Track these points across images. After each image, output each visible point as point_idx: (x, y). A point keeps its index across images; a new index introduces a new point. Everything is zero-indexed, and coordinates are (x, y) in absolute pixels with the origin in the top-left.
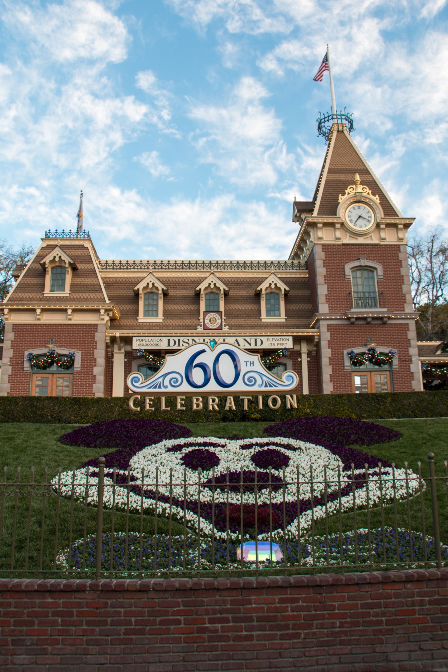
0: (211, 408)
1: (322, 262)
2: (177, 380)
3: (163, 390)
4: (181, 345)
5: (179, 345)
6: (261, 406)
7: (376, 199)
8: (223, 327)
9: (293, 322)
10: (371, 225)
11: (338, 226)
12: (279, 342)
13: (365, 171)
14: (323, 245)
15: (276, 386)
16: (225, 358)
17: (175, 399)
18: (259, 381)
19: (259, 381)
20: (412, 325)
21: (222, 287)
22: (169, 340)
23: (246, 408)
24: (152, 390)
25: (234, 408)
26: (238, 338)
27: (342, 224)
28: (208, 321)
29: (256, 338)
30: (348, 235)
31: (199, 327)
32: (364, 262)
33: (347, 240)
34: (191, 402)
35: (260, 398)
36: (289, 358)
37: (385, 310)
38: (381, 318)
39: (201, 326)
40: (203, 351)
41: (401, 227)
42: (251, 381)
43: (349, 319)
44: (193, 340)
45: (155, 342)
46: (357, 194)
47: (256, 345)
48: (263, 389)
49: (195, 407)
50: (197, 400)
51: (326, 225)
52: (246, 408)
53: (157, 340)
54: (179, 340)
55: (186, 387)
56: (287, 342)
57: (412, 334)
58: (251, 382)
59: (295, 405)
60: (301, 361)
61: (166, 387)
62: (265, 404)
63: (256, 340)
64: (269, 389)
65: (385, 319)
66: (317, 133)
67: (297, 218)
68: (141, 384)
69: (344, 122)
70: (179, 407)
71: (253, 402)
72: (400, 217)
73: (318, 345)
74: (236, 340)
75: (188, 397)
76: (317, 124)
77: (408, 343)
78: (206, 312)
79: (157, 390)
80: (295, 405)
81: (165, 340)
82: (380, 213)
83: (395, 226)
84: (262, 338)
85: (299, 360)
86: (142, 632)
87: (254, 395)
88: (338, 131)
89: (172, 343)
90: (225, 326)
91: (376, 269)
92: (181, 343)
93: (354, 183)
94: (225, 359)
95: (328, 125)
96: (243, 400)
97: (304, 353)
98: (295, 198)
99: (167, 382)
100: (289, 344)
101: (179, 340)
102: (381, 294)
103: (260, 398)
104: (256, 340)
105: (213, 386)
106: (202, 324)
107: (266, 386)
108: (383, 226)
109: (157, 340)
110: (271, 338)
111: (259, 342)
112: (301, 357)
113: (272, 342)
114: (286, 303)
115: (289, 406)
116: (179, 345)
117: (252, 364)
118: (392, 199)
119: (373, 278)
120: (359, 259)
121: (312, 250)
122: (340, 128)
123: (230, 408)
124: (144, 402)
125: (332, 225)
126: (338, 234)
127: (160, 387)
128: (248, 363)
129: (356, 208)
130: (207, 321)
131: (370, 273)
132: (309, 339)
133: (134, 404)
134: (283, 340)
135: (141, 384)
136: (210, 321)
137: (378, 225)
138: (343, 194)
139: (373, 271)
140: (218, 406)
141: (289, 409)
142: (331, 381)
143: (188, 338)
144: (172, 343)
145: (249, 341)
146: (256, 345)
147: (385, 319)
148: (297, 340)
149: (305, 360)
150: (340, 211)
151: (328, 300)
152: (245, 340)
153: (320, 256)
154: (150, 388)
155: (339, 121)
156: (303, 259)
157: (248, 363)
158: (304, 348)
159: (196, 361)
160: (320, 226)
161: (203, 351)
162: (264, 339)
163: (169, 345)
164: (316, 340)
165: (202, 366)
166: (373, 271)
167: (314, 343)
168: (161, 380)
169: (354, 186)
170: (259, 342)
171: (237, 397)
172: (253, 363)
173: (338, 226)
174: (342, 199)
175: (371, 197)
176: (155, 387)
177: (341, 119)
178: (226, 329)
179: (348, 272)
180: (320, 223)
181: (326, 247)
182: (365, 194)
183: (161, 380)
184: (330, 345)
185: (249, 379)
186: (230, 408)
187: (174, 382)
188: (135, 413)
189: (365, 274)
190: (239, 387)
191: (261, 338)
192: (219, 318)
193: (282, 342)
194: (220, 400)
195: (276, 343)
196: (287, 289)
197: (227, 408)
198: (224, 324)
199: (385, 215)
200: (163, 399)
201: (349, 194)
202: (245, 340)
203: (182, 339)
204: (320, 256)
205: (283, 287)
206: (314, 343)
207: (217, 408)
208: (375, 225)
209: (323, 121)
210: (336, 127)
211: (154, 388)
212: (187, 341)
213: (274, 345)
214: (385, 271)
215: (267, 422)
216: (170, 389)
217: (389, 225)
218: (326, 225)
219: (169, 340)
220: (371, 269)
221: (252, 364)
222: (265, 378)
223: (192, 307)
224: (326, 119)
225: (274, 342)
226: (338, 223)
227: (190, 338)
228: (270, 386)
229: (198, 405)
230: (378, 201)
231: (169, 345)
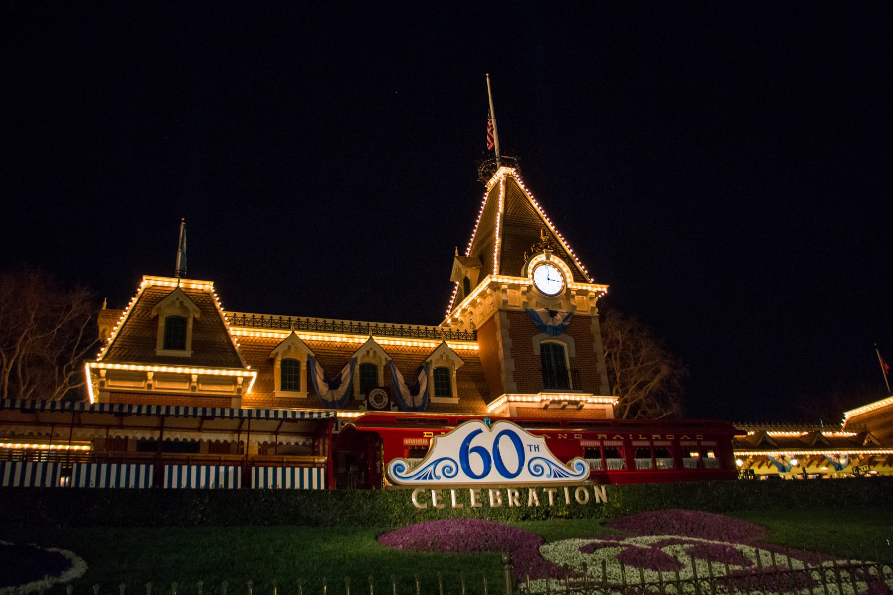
0: (511, 503)
1: (507, 331)
2: (451, 469)
3: (434, 481)
6: (567, 501)
8: (392, 408)
15: (566, 477)
16: (505, 439)
17: (469, 491)
18: (547, 471)
19: (547, 471)
23: (551, 502)
24: (421, 481)
25: (537, 504)
28: (373, 399)
34: (487, 497)
35: (566, 490)
39: (364, 405)
40: (479, 431)
42: (537, 471)
48: (552, 479)
49: (492, 504)
50: (494, 494)
52: (551, 502)
55: (462, 478)
58: (538, 471)
59: (605, 500)
61: (438, 478)
62: (572, 498)
64: (558, 479)
65: (582, 403)
68: (407, 473)
70: (473, 503)
71: (558, 495)
75: (463, 492)
79: (427, 481)
80: (605, 500)
87: (540, 489)
90: (394, 406)
94: (506, 444)
96: (547, 494)
99: (439, 472)
102: (574, 372)
103: (566, 490)
105: (494, 477)
106: (365, 402)
107: (555, 476)
115: (598, 500)
117: (537, 448)
123: (534, 504)
124: (430, 498)
127: (430, 478)
128: (533, 448)
130: (371, 399)
133: (418, 500)
135: (407, 473)
136: (375, 398)
140: (519, 500)
141: (598, 504)
154: (418, 479)
157: (533, 448)
159: (472, 445)
161: (479, 431)
165: (480, 450)
168: (431, 468)
171: (523, 491)
172: (538, 448)
176: (425, 478)
183: (431, 468)
185: (535, 467)
186: (534, 504)
187: (448, 472)
188: (421, 512)
190: (525, 477)
192: (387, 395)
194: (520, 494)
197: (530, 503)
198: (392, 403)
200: (453, 492)
207: (517, 504)
211: (423, 479)
216: (444, 480)
221: (537, 448)
222: (553, 467)
228: (560, 476)
229: (496, 501)
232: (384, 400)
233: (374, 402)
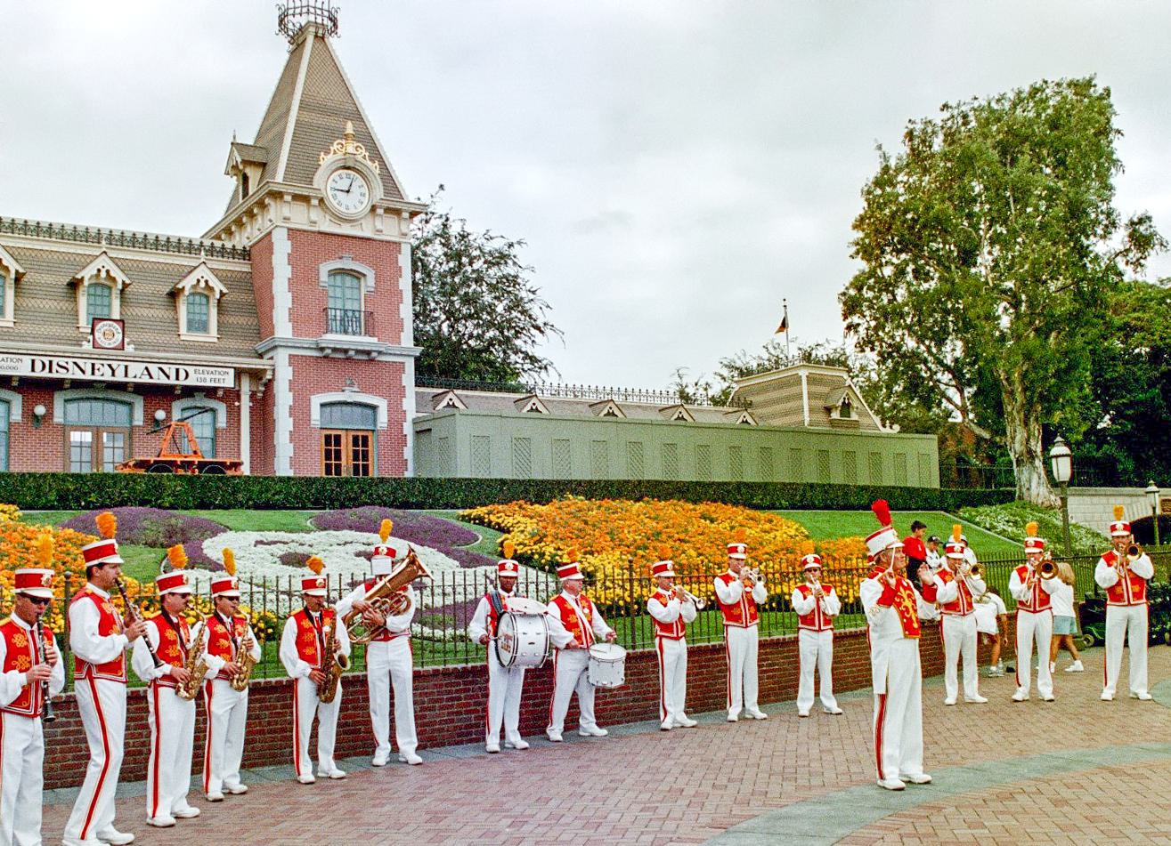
4: (54, 370)
5: (50, 371)
7: (374, 167)
9: (232, 344)
10: (364, 207)
11: (315, 202)
12: (213, 376)
13: (358, 116)
14: (289, 229)
20: (410, 366)
21: (120, 277)
22: (33, 361)
26: (149, 366)
27: (321, 200)
29: (177, 367)
30: (328, 217)
31: (84, 343)
32: (348, 264)
33: (327, 226)
36: (221, 399)
37: (375, 340)
38: (368, 353)
41: (406, 215)
43: (322, 349)
44: (75, 363)
45: (9, 364)
46: (348, 156)
47: (177, 378)
51: (296, 197)
53: (12, 360)
54: (51, 362)
56: (226, 377)
57: (409, 377)
60: (239, 407)
63: (177, 370)
65: (374, 354)
66: (278, 28)
67: (234, 169)
69: (327, 22)
72: (406, 200)
73: (269, 385)
74: (147, 368)
76: (277, 13)
77: (401, 391)
78: (95, 321)
81: (27, 360)
82: (379, 193)
83: (397, 212)
84: (188, 368)
85: (237, 404)
86: (433, 709)
88: (316, 36)
89: (38, 366)
91: (364, 275)
92: (55, 367)
93: (346, 137)
95: (297, 21)
97: (246, 394)
98: (234, 138)
100: (228, 381)
101: (51, 362)
104: (177, 370)
108: (380, 211)
109: (12, 360)
110: (201, 368)
111: (182, 375)
112: (239, 400)
113: (202, 376)
114: (220, 313)
116: (50, 371)
118: (392, 161)
119: (359, 289)
120: (341, 258)
121: (270, 233)
122: (320, 32)
125: (305, 199)
126: (315, 214)
129: (344, 176)
131: (355, 281)
132: (256, 375)
134: (220, 373)
137: (373, 209)
138: (327, 153)
139: (359, 279)
142: (291, 441)
143: (66, 360)
144: (38, 366)
145: (167, 371)
146: (177, 378)
147: (374, 354)
148: (239, 373)
149: (245, 404)
150: (318, 181)
151: (294, 317)
152: (160, 369)
153: (282, 247)
155: (319, 20)
156: (241, 240)
158: (246, 387)
160: (287, 198)
162: (191, 370)
163: (33, 370)
164: (269, 376)
166: (359, 279)
167: (264, 381)
169: (344, 142)
170: (182, 375)
173: (315, 202)
174: (326, 160)
175: (369, 163)
177: (322, 15)
178: (129, 349)
179: (324, 277)
180: (289, 194)
181: (293, 233)
182: (359, 158)
184: (292, 385)
189: (348, 280)
191: (186, 367)
192: (120, 331)
193: (217, 376)
195: (208, 377)
196: (225, 291)
198: (126, 340)
199: (386, 194)
201: (335, 153)
202: (160, 369)
203: (55, 360)
204: (282, 247)
205: (218, 286)
206: (264, 381)
208: (369, 208)
209: (291, 12)
210: (312, 29)
212: (65, 365)
213: (205, 380)
214: (378, 279)
215: (347, 535)
217: (388, 210)
218: (296, 197)
219: (33, 361)
220: (358, 276)
223: (65, 305)
224: (298, 11)
225: (206, 376)
226: (316, 197)
227: (70, 360)
230: (378, 171)
231: (33, 370)
232: (116, 335)
233: (102, 338)
